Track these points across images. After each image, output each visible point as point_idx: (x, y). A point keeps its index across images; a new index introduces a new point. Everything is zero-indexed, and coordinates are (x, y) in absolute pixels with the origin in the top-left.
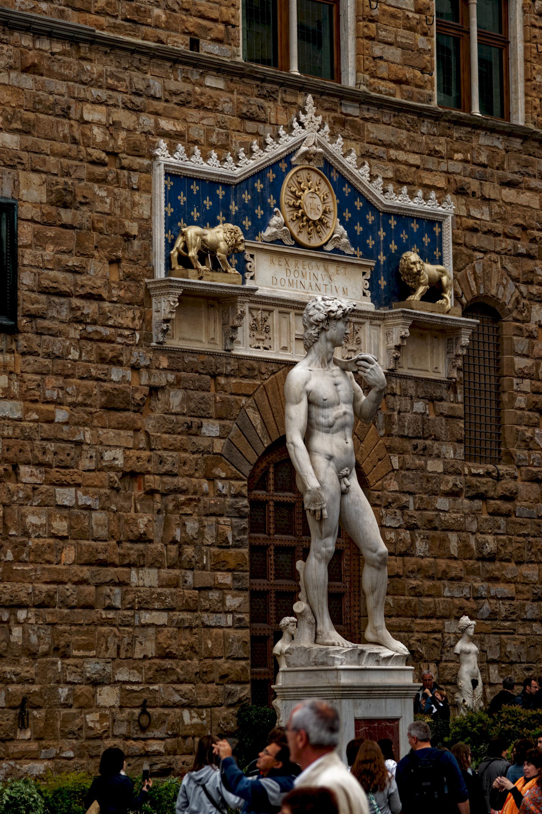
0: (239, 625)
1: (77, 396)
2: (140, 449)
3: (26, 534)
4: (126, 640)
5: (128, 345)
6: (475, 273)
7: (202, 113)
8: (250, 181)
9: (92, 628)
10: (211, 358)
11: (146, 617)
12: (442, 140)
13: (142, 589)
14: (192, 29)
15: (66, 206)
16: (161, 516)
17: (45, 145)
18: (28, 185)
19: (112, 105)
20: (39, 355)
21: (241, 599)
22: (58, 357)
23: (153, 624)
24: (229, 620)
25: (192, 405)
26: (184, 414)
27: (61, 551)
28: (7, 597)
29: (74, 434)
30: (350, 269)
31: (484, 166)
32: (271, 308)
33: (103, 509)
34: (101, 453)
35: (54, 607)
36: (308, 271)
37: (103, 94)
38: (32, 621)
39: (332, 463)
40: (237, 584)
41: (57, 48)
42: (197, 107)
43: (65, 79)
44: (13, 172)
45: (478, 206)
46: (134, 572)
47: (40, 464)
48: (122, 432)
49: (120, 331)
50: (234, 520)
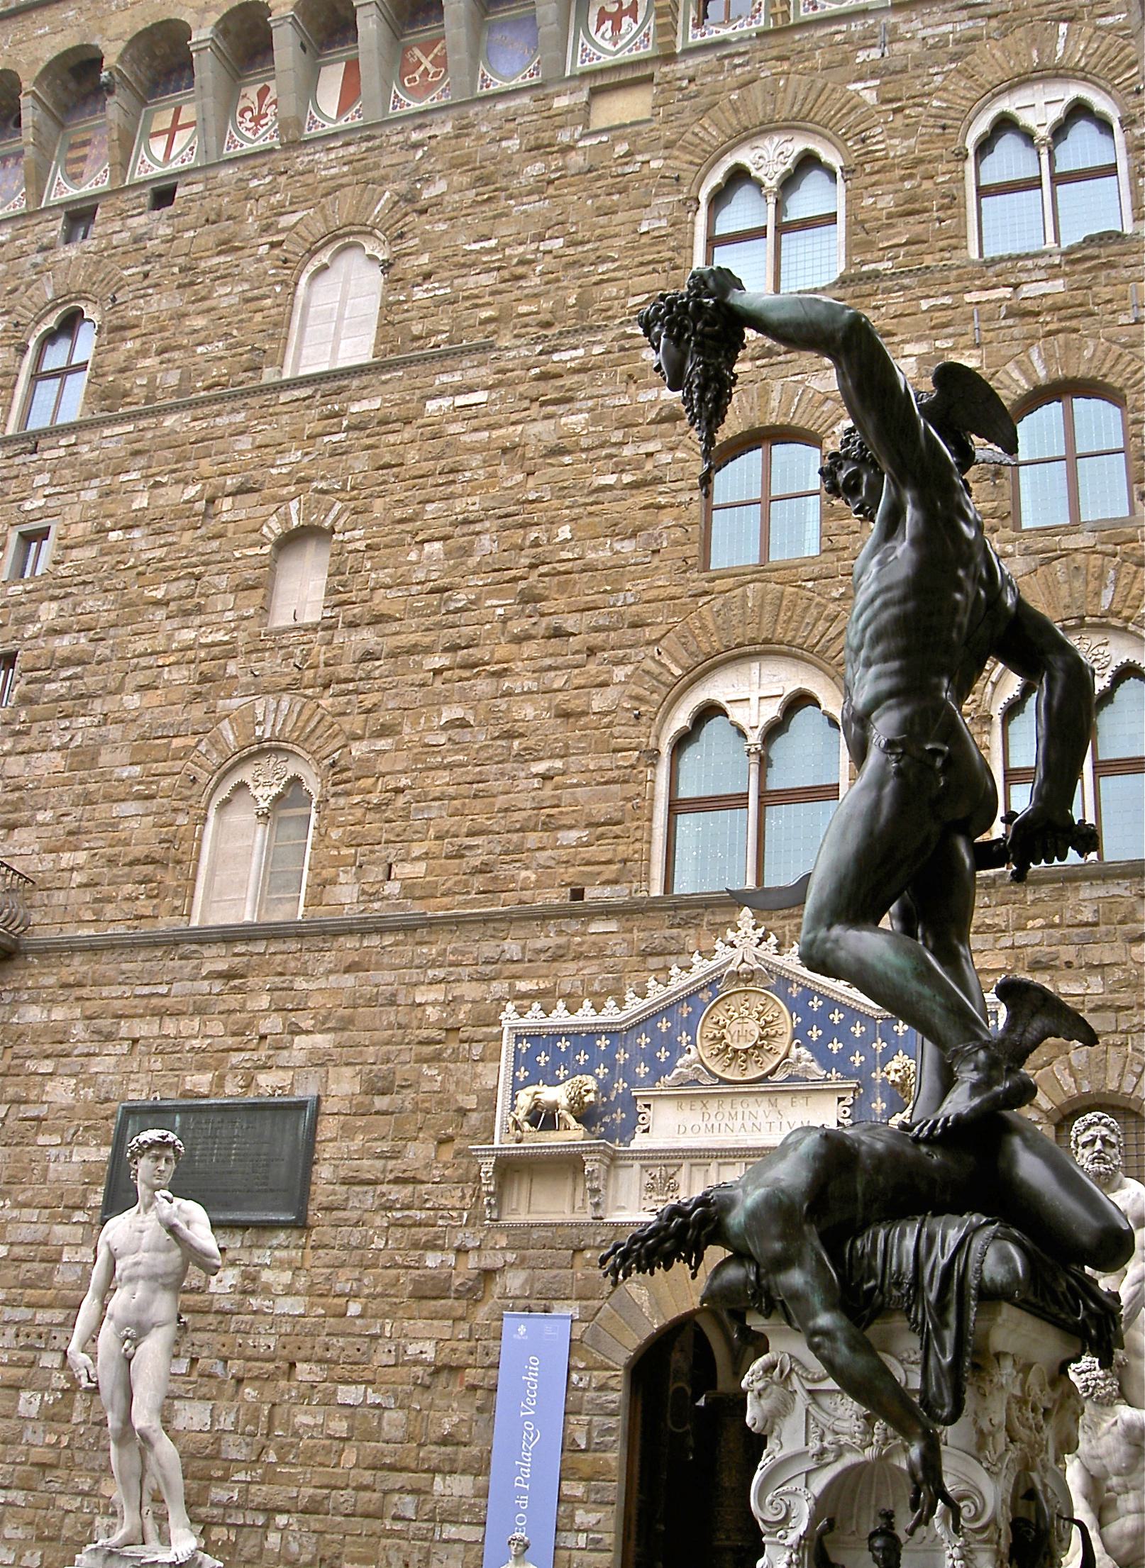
0: (595, 1545)
1: (375, 1287)
2: (459, 1340)
3: (296, 1434)
4: (416, 1556)
5: (454, 1227)
6: (1070, 1067)
7: (581, 964)
8: (650, 1022)
9: (373, 1540)
10: (574, 1230)
11: (451, 1531)
12: (1002, 909)
13: (445, 1499)
14: (569, 880)
15: (382, 1093)
16: (486, 1415)
17: (364, 1037)
18: (338, 1081)
19: (453, 981)
20: (333, 1248)
21: (599, 1515)
22: (357, 1248)
23: (460, 1540)
24: (582, 1539)
25: (538, 1286)
26: (527, 1297)
27: (340, 1453)
28: (260, 1500)
29: (368, 1327)
30: (814, 1098)
31: (1096, 924)
32: (676, 1161)
33: (401, 1407)
34: (404, 1347)
35: (327, 1514)
36: (740, 1110)
37: (440, 973)
38: (295, 1527)
39: (112, 1323)
40: (593, 1497)
41: (389, 939)
42: (576, 958)
43: (394, 968)
44: (322, 1070)
45: (1077, 979)
46: (438, 1478)
47: (319, 1361)
48: (435, 1322)
49: (440, 1213)
50: (596, 1418)
